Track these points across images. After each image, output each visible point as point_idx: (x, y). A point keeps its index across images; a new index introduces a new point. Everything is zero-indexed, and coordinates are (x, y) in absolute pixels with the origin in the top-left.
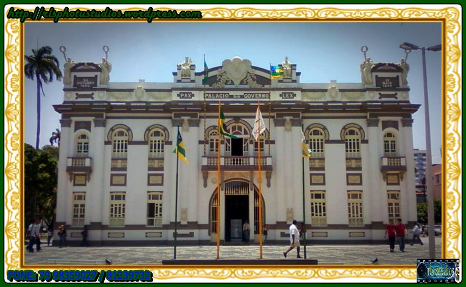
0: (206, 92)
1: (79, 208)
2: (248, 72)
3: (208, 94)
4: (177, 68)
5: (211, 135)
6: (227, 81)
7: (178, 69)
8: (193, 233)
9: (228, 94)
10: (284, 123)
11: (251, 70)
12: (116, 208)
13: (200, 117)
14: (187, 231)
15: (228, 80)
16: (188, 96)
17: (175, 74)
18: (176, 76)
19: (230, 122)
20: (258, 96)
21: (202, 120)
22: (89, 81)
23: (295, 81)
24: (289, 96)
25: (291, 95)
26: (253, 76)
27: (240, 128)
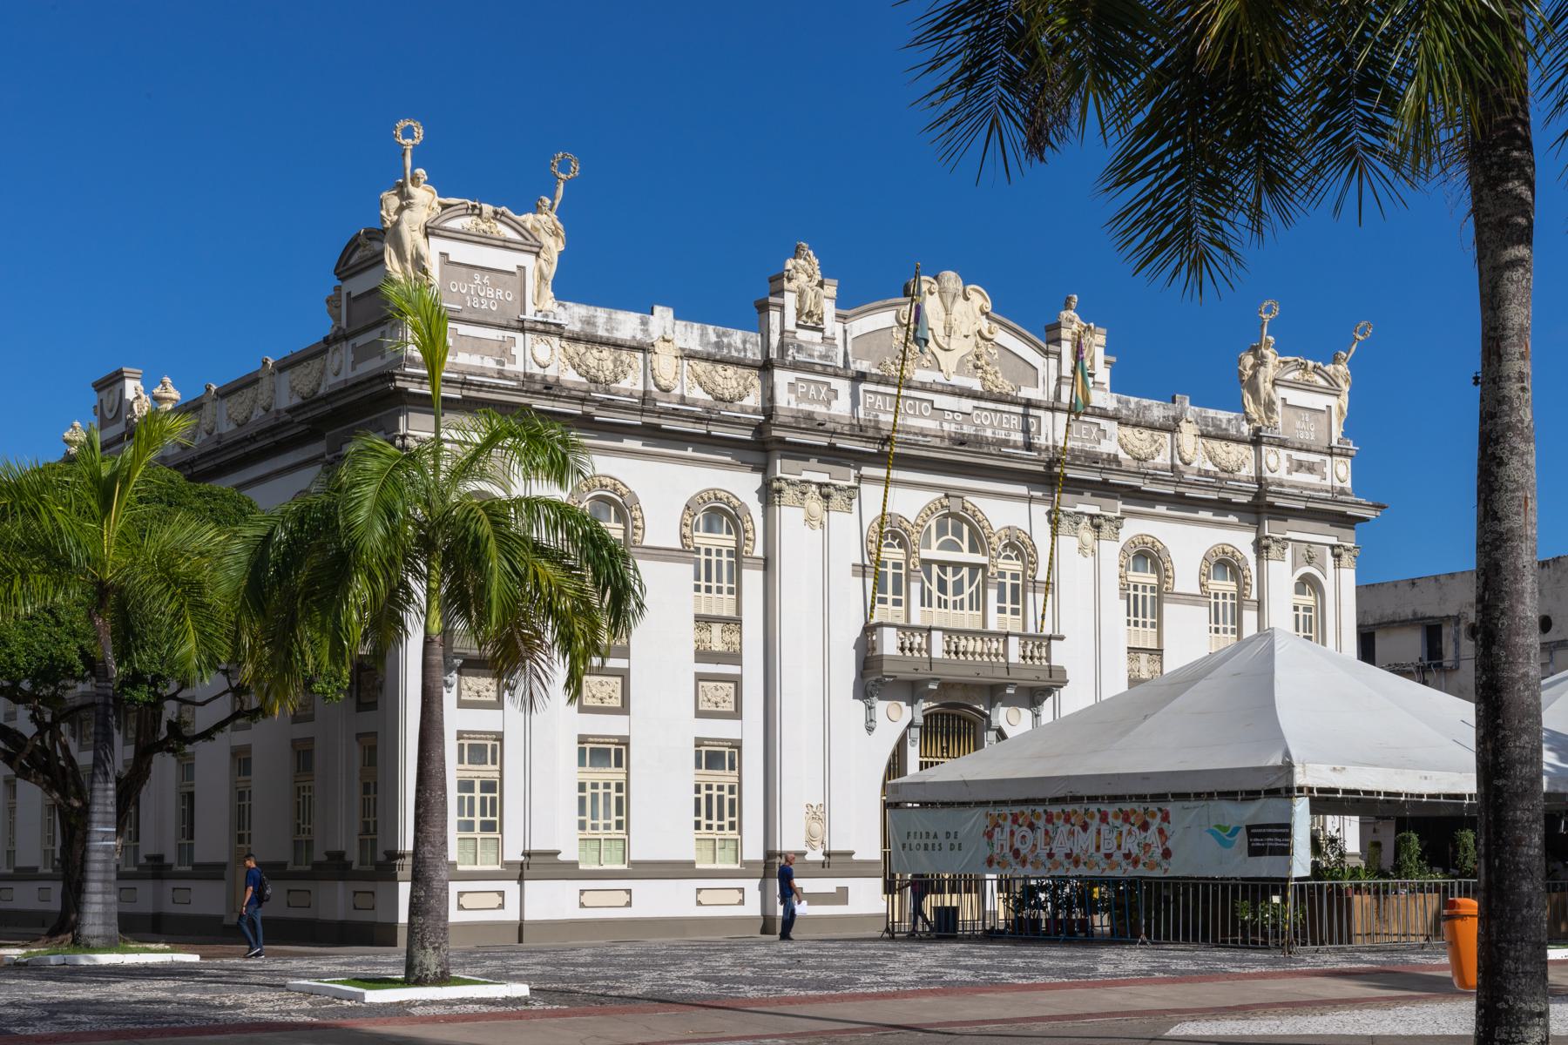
1: (477, 795)
8: (846, 889)
12: (595, 797)
14: (828, 885)
20: (1009, 421)
22: (495, 286)
24: (1089, 432)
25: (1095, 429)
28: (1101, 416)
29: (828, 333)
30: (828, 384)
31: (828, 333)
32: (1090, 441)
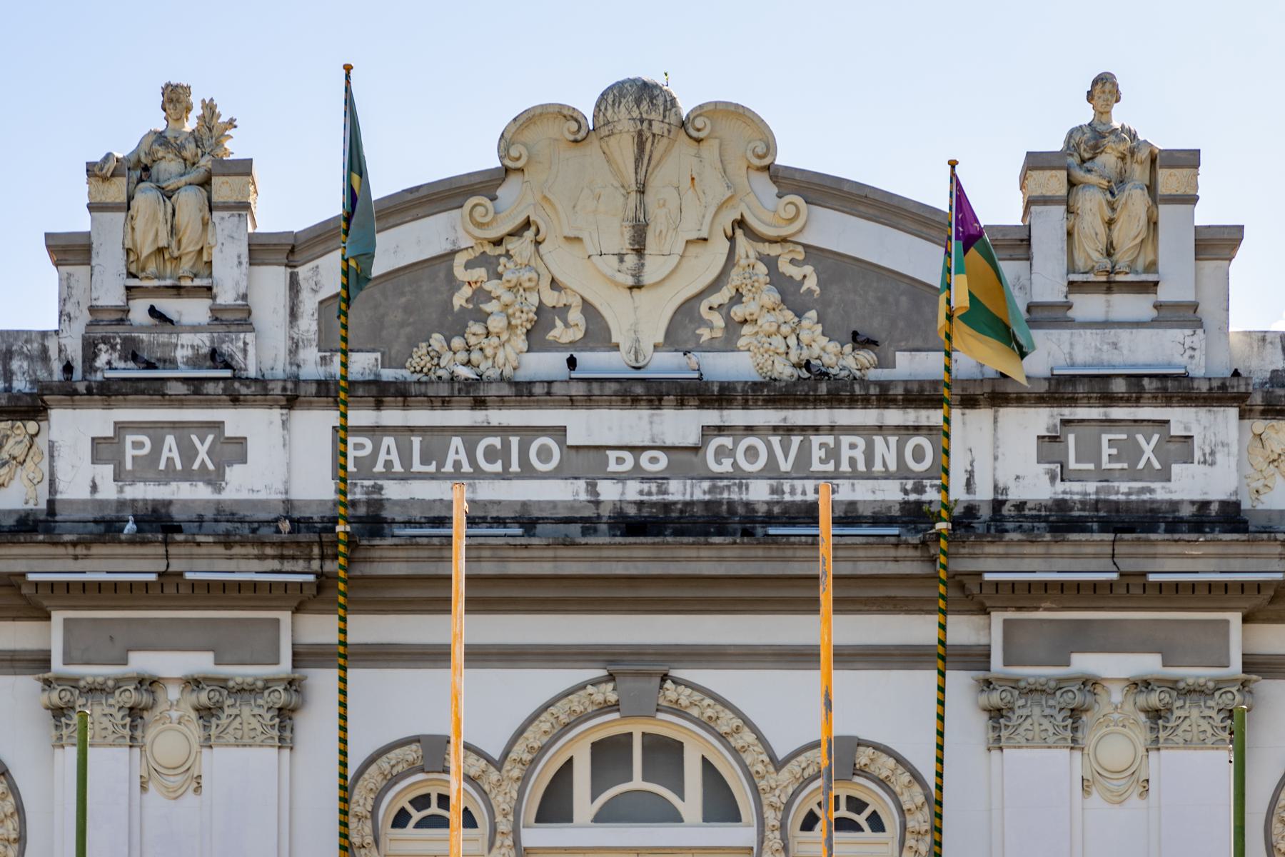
0: (359, 417)
2: (741, 223)
3: (375, 431)
4: (80, 191)
5: (401, 819)
6: (543, 319)
7: (92, 207)
9: (559, 432)
10: (1075, 713)
11: (768, 211)
13: (301, 656)
15: (551, 298)
16: (188, 453)
17: (68, 251)
18: (80, 272)
19: (577, 703)
21: (323, 681)
23: (1184, 315)
25: (1148, 446)
26: (785, 267)
27: (665, 755)
28: (1168, 399)
29: (226, 297)
30: (218, 426)
31: (226, 297)
32: (1132, 475)
